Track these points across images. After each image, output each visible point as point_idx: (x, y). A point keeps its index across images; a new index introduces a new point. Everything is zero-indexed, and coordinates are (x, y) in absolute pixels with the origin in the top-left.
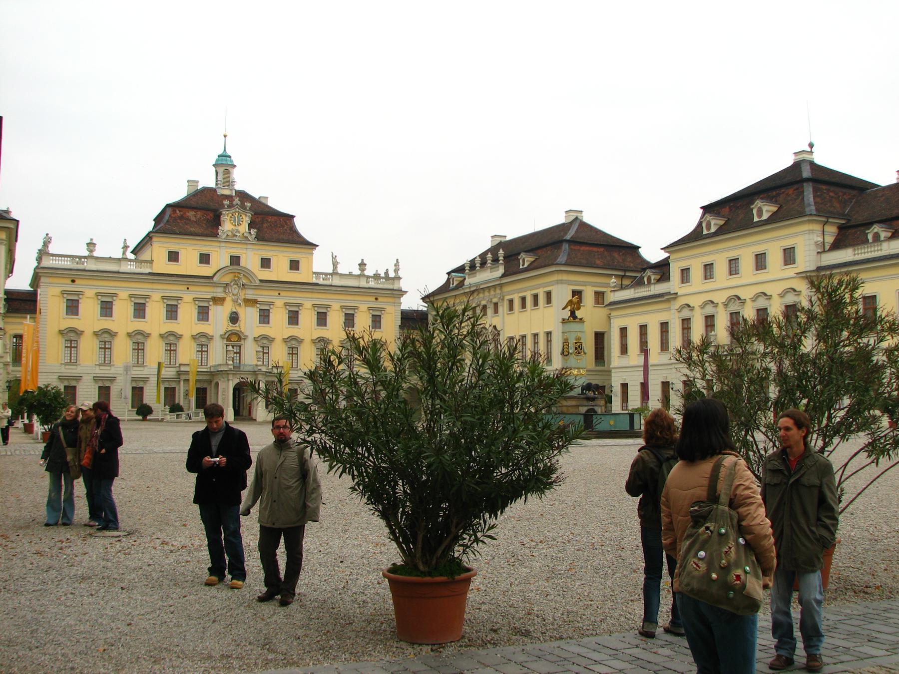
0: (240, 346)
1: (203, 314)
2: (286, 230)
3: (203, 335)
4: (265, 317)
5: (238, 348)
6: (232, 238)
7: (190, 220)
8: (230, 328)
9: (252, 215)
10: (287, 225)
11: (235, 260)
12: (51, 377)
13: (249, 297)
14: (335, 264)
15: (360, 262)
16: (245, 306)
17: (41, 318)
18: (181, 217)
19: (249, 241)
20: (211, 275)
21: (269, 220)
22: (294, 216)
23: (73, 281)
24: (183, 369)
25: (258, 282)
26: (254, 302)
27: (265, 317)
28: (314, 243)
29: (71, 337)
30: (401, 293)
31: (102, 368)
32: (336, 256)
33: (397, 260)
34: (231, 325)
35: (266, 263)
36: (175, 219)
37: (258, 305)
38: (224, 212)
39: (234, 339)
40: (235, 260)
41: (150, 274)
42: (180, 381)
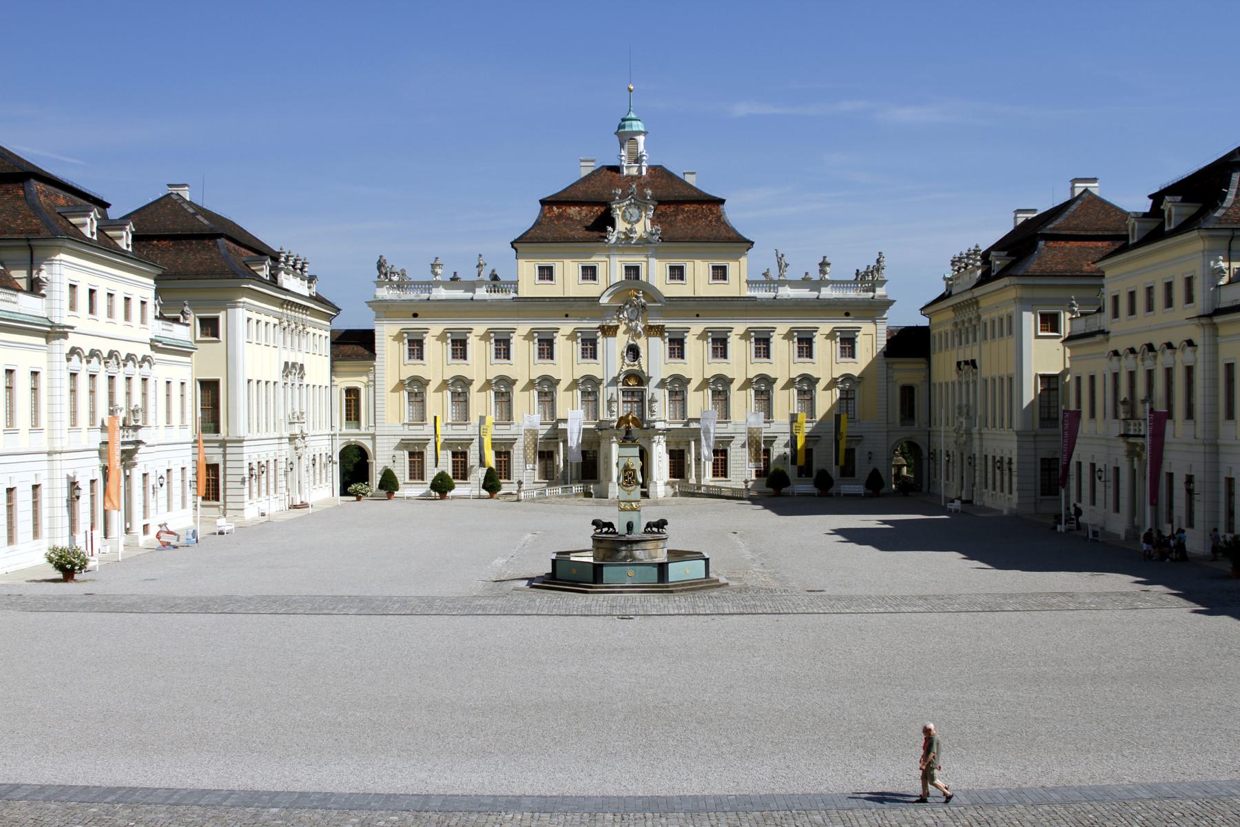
0: (643, 392)
1: (590, 348)
2: (711, 221)
3: (589, 379)
4: (677, 347)
5: (640, 394)
6: (627, 243)
7: (572, 219)
8: (625, 368)
9: (654, 205)
10: (713, 213)
11: (633, 271)
12: (391, 441)
13: (652, 322)
14: (782, 266)
15: (821, 261)
16: (648, 336)
17: (377, 362)
18: (560, 216)
19: (651, 243)
20: (598, 296)
21: (686, 209)
22: (722, 201)
23: (415, 315)
24: (561, 426)
25: (664, 301)
26: (659, 331)
27: (677, 347)
28: (747, 237)
29: (416, 388)
30: (886, 304)
31: (454, 427)
32: (783, 256)
33: (880, 253)
34: (627, 361)
35: (677, 273)
36: (551, 220)
37: (666, 334)
38: (614, 206)
39: (635, 381)
40: (633, 271)
41: (513, 298)
42: (558, 443)
